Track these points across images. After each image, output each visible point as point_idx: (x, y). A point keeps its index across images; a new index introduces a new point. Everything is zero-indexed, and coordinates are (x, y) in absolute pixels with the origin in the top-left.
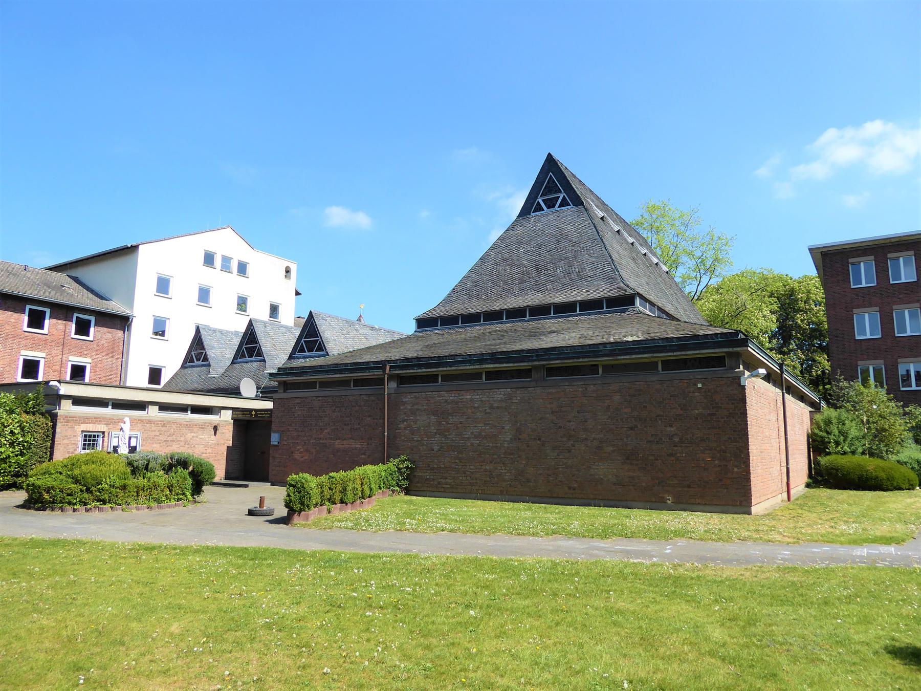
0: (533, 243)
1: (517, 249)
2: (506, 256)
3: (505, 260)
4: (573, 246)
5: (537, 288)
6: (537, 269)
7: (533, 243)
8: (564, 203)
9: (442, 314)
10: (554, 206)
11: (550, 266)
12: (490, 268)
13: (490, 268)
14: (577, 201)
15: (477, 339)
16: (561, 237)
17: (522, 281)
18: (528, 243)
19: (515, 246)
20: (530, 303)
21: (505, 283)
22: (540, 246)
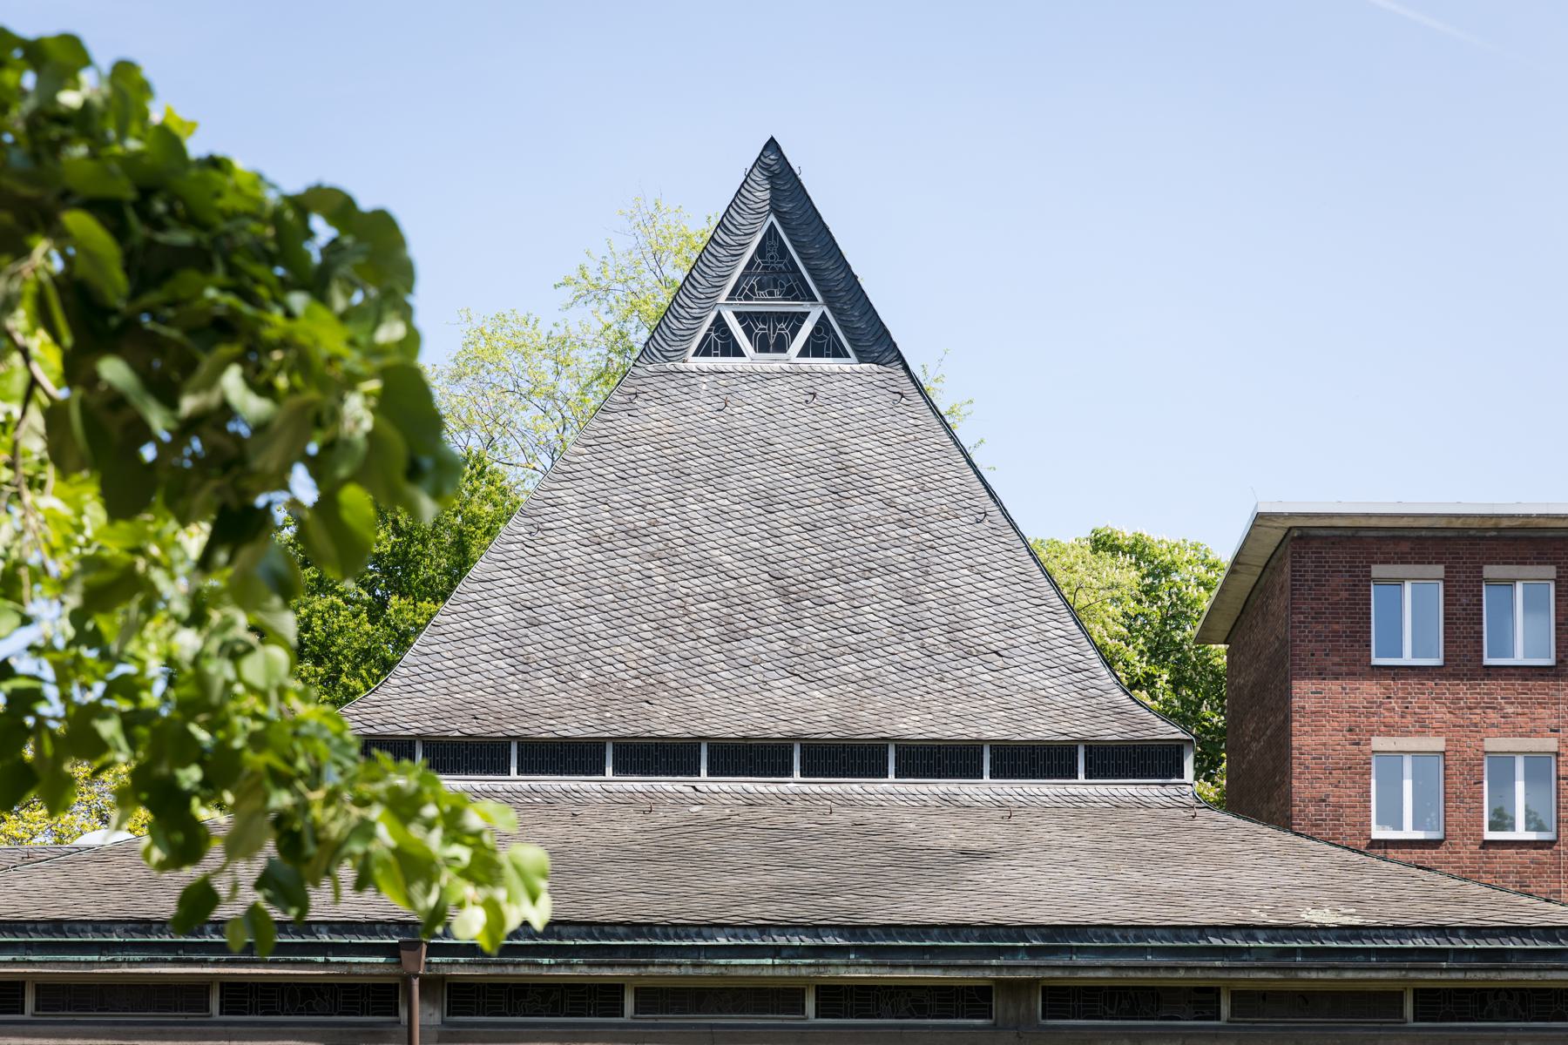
1: (675, 496)
2: (633, 517)
5: (796, 666)
6: (784, 593)
8: (821, 345)
9: (429, 727)
10: (781, 346)
11: (830, 588)
13: (575, 556)
14: (875, 342)
15: (672, 849)
16: (843, 480)
17: (732, 635)
19: (656, 485)
20: (801, 727)
22: (768, 502)
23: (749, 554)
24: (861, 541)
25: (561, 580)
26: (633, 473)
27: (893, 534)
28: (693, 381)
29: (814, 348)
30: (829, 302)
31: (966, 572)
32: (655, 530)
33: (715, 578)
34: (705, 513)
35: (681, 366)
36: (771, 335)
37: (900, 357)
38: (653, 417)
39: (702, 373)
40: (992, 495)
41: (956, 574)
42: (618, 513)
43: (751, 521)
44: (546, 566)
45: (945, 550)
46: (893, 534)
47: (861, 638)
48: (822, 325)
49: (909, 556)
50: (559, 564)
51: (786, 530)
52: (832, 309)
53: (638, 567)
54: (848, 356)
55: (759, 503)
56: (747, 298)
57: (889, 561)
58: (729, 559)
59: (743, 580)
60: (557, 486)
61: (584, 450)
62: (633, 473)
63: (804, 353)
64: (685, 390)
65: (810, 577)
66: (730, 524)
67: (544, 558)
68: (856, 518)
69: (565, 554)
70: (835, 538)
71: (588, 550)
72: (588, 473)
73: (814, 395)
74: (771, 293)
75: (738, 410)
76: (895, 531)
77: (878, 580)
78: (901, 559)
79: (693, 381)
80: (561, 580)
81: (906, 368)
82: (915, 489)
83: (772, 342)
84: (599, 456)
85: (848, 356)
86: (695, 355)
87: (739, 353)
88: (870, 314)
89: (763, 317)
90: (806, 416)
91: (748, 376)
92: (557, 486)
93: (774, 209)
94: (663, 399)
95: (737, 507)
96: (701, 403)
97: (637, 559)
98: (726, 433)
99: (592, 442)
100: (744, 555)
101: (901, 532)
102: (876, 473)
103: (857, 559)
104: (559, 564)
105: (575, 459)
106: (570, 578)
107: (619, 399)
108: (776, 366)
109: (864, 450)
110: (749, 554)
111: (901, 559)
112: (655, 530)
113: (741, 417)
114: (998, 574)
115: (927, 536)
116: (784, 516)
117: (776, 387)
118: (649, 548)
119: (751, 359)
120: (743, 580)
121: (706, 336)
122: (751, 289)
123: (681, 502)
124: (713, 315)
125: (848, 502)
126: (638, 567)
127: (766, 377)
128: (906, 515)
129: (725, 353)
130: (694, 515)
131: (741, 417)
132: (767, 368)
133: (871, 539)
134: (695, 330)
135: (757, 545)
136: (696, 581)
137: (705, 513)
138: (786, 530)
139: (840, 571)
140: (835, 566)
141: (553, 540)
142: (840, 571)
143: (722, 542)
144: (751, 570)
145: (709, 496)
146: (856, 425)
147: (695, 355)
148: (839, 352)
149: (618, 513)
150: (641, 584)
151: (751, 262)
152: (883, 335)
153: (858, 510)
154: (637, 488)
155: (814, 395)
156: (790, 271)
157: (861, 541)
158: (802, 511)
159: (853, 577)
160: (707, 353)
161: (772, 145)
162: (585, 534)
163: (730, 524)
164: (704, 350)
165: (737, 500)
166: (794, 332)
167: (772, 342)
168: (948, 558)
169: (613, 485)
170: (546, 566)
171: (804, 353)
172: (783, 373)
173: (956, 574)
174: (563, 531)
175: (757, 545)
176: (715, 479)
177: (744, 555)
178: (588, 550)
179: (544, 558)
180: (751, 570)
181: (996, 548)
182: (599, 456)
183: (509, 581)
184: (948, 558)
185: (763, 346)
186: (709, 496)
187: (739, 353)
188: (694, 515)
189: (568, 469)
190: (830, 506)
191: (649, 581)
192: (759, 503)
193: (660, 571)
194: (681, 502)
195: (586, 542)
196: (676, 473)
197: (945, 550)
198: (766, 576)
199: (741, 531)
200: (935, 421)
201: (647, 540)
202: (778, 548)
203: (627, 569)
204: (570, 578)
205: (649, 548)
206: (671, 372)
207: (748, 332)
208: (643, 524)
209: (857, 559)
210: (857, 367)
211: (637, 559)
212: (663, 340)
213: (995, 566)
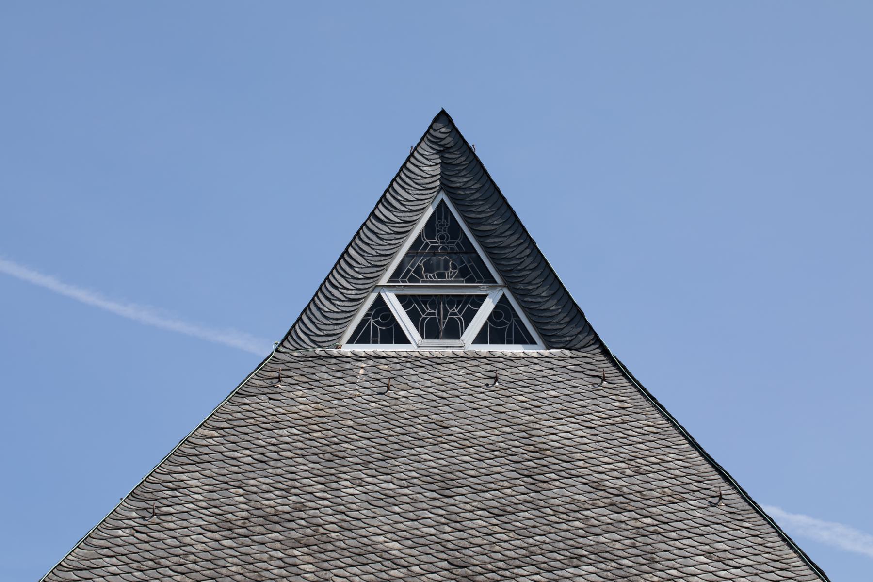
2: (273, 501)
3: (272, 519)
10: (454, 332)
13: (198, 542)
16: (536, 463)
19: (303, 468)
22: (445, 486)
23: (422, 541)
24: (564, 526)
25: (180, 569)
26: (275, 456)
27: (604, 519)
28: (348, 366)
29: (493, 333)
30: (509, 284)
31: (702, 559)
32: (302, 514)
33: (379, 566)
34: (364, 497)
35: (334, 352)
36: (441, 319)
37: (597, 340)
38: (299, 399)
39: (358, 358)
40: (726, 478)
41: (690, 562)
42: (255, 497)
43: (424, 506)
44: (162, 553)
45: (673, 535)
46: (604, 519)
49: (628, 542)
50: (178, 551)
51: (468, 515)
52: (513, 293)
53: (280, 555)
54: (533, 342)
55: (433, 487)
57: (603, 547)
58: (397, 545)
59: (416, 569)
60: (180, 469)
61: (215, 433)
62: (275, 456)
63: (480, 339)
64: (339, 374)
65: (501, 565)
66: (397, 509)
67: (160, 545)
68: (557, 502)
69: (187, 540)
70: (531, 523)
71: (216, 536)
72: (219, 456)
73: (496, 379)
74: (441, 276)
75: (402, 393)
76: (608, 517)
77: (590, 568)
78: (618, 545)
79: (348, 366)
80: (180, 569)
81: (605, 352)
82: (628, 472)
84: (232, 439)
87: (403, 339)
88: (561, 293)
89: (432, 301)
90: (487, 400)
92: (180, 469)
93: (445, 186)
94: (311, 383)
95: (406, 491)
96: (359, 387)
97: (278, 545)
98: (390, 417)
99: (225, 425)
100: (416, 541)
101: (615, 516)
102: (578, 456)
103: (561, 545)
104: (178, 551)
105: (204, 442)
106: (190, 566)
107: (257, 382)
108: (448, 351)
109: (563, 432)
110: (422, 541)
111: (618, 545)
112: (302, 514)
113: (408, 400)
114: (745, 561)
115: (649, 521)
116: (463, 500)
117: (447, 372)
118: (293, 534)
120: (416, 569)
122: (418, 271)
123: (334, 485)
124: (373, 297)
125: (545, 485)
126: (280, 555)
127: (436, 362)
128: (621, 499)
129: (386, 339)
130: (350, 499)
131: (408, 400)
132: (436, 352)
133: (577, 524)
134: (351, 315)
135: (432, 531)
136: (355, 570)
137: (364, 497)
138: (468, 515)
139: (540, 558)
141: (172, 525)
142: (540, 558)
143: (386, 528)
144: (424, 558)
145: (370, 480)
146: (549, 408)
148: (524, 339)
149: (255, 497)
150: (283, 572)
152: (576, 314)
153: (557, 494)
154: (279, 471)
155: (496, 379)
156: (466, 245)
157: (564, 526)
158: (487, 495)
159: (558, 565)
160: (364, 340)
161: (443, 117)
162: (212, 519)
163: (397, 509)
165: (405, 483)
166: (469, 317)
168: (677, 544)
169: (249, 468)
170: (162, 553)
171: (480, 339)
172: (456, 358)
173: (690, 562)
174: (185, 516)
175: (432, 531)
176: (379, 461)
178: (216, 536)
179: (160, 545)
180: (424, 558)
181: (738, 533)
182: (232, 439)
183: (113, 569)
184: (677, 544)
185: (430, 332)
186: (370, 480)
187: (403, 339)
188: (350, 499)
189: (194, 451)
190: (523, 489)
191: (294, 570)
192: (433, 487)
193: (307, 558)
194: (334, 485)
195: (213, 527)
196: (328, 456)
197: (673, 535)
198: (445, 564)
199: (411, 515)
200: (646, 405)
201: (292, 525)
202: (458, 534)
203: (265, 557)
204: (190, 566)
205: (293, 534)
206: (321, 357)
207: (414, 317)
208: (287, 509)
209: (561, 545)
210: (546, 352)
211: (278, 545)
213: (739, 552)
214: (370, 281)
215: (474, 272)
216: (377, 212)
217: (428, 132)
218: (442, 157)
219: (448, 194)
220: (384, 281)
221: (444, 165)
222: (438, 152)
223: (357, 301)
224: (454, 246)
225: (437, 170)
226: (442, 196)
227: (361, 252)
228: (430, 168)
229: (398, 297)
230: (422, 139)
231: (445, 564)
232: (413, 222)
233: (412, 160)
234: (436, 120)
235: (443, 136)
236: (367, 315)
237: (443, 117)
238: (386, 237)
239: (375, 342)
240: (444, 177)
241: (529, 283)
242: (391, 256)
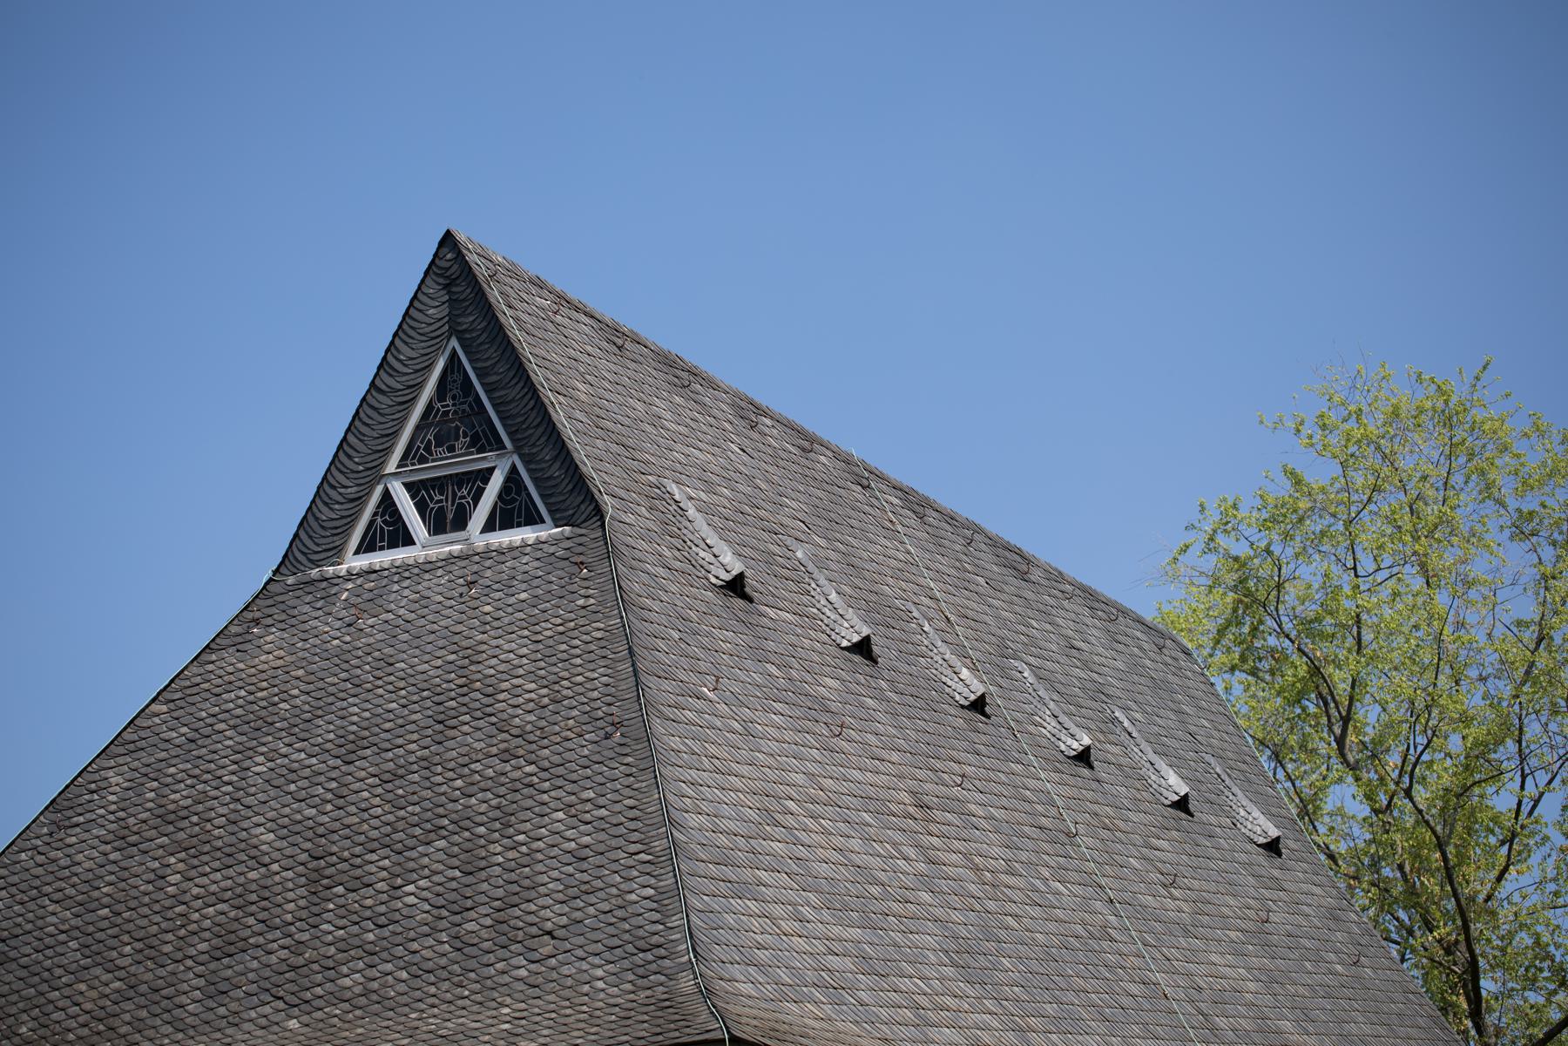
0: (325, 731)
2: (179, 797)
3: (168, 818)
4: (507, 755)
7: (325, 731)
8: (509, 513)
10: (461, 522)
11: (379, 864)
12: (86, 860)
13: (86, 860)
14: (575, 499)
17: (228, 945)
18: (299, 728)
21: (148, 950)
30: (518, 449)
36: (445, 507)
47: (386, 932)
48: (512, 478)
54: (543, 521)
56: (423, 460)
63: (489, 527)
74: (451, 449)
83: (450, 516)
85: (543, 521)
86: (357, 552)
87: (409, 541)
89: (438, 484)
91: (428, 567)
94: (289, 621)
108: (456, 548)
116: (363, 768)
119: (425, 546)
121: (371, 523)
124: (379, 489)
129: (393, 545)
140: (396, 831)
147: (357, 552)
148: (533, 519)
151: (429, 407)
152: (579, 482)
164: (367, 546)
167: (450, 516)
171: (489, 527)
177: (288, 830)
185: (438, 525)
187: (409, 541)
207: (421, 507)
212: (315, 538)
214: (375, 473)
215: (485, 440)
216: (378, 382)
217: (433, 262)
218: (449, 292)
219: (460, 340)
220: (391, 467)
221: (452, 302)
222: (446, 286)
223: (359, 501)
224: (466, 407)
225: (445, 310)
226: (454, 343)
227: (361, 437)
228: (436, 311)
229: (405, 484)
230: (427, 273)
231: (304, 857)
232: (420, 386)
233: (416, 304)
234: (442, 243)
235: (448, 265)
236: (375, 514)
237: (448, 239)
238: (388, 411)
239: (382, 548)
240: (452, 319)
241: (534, 445)
242: (395, 434)
